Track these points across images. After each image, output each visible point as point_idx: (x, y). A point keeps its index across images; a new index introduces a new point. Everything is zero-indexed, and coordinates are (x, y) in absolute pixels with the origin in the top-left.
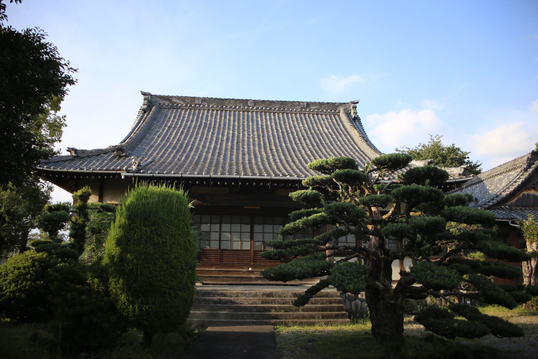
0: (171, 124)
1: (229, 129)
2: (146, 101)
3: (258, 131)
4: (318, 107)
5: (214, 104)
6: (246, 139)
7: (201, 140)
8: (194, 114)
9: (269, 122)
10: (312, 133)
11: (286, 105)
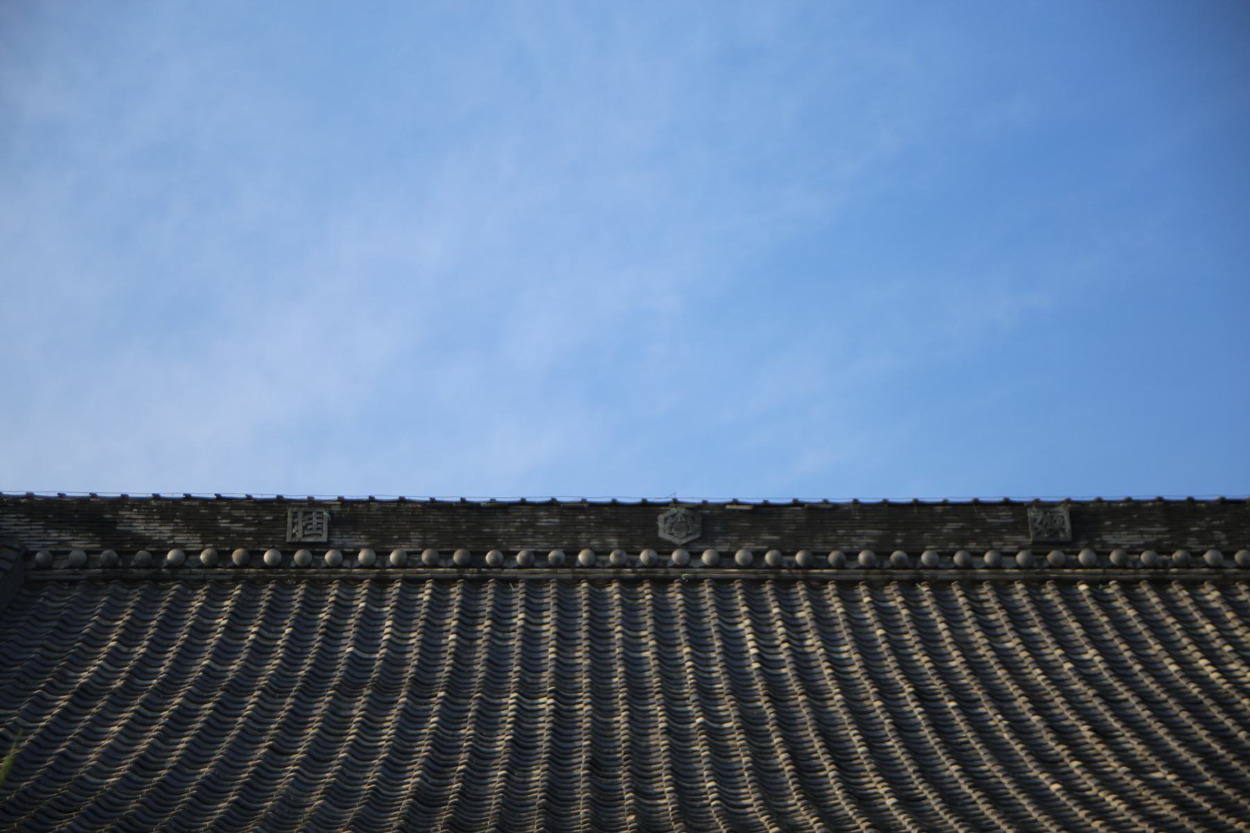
0: (103, 677)
1: (529, 690)
3: (741, 689)
4: (1157, 531)
5: (416, 538)
6: (659, 741)
9: (812, 642)
10: (1146, 698)
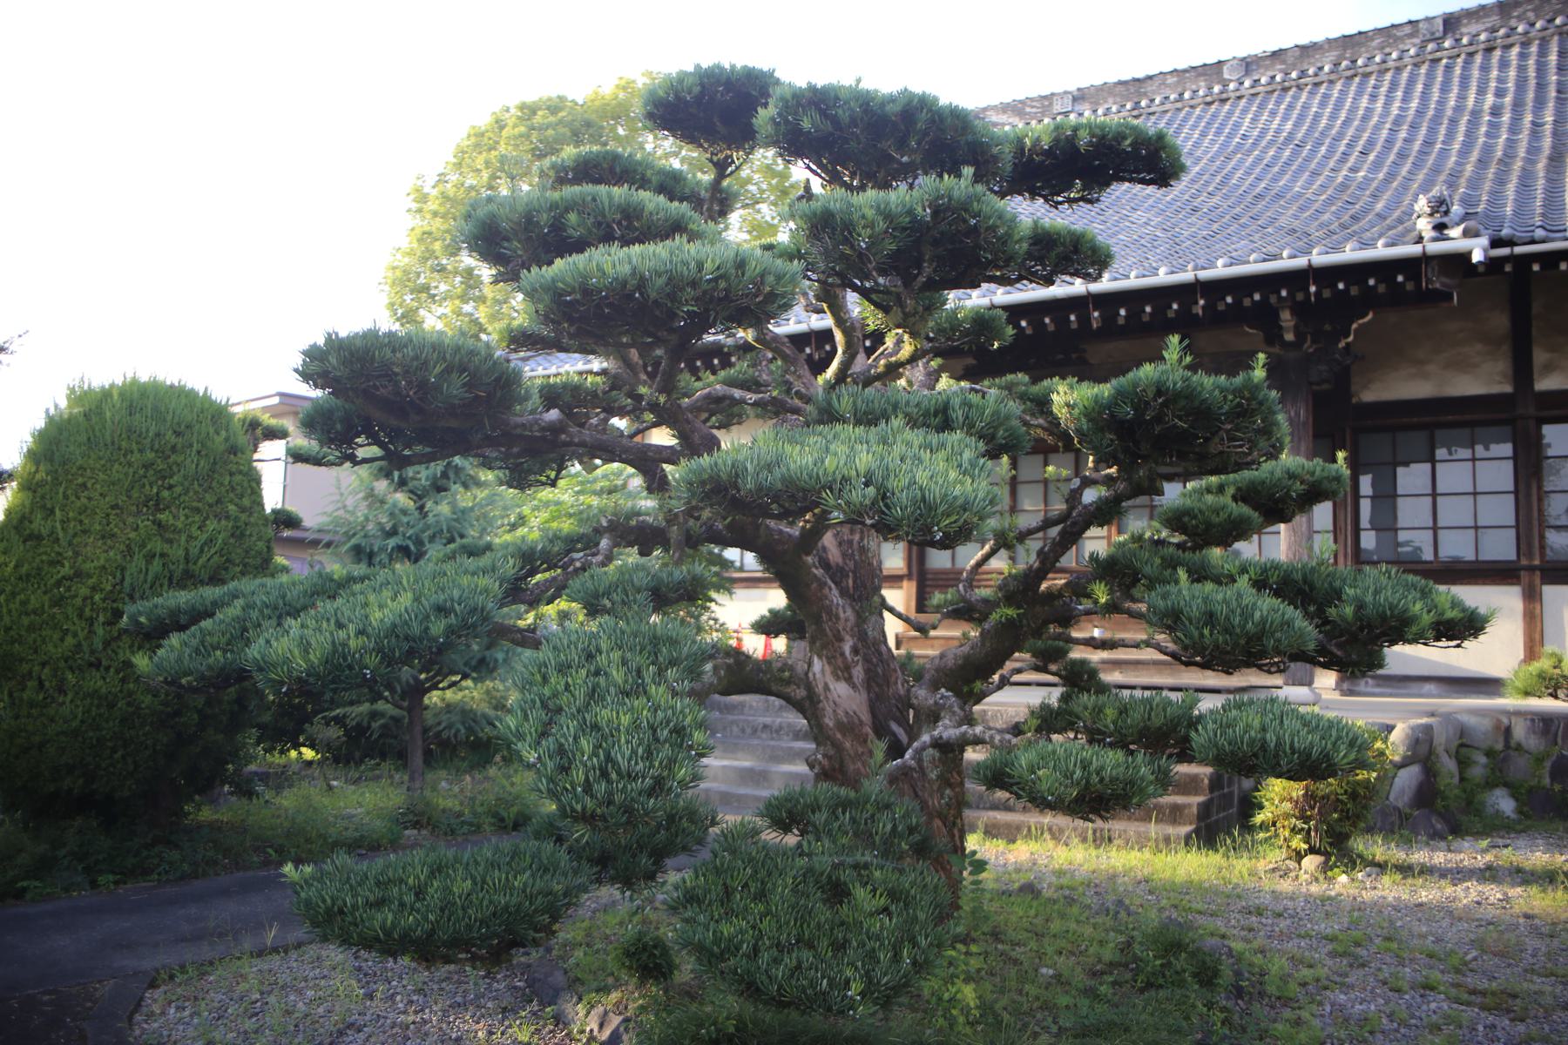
5: (1111, 100)
11: (1360, 44)
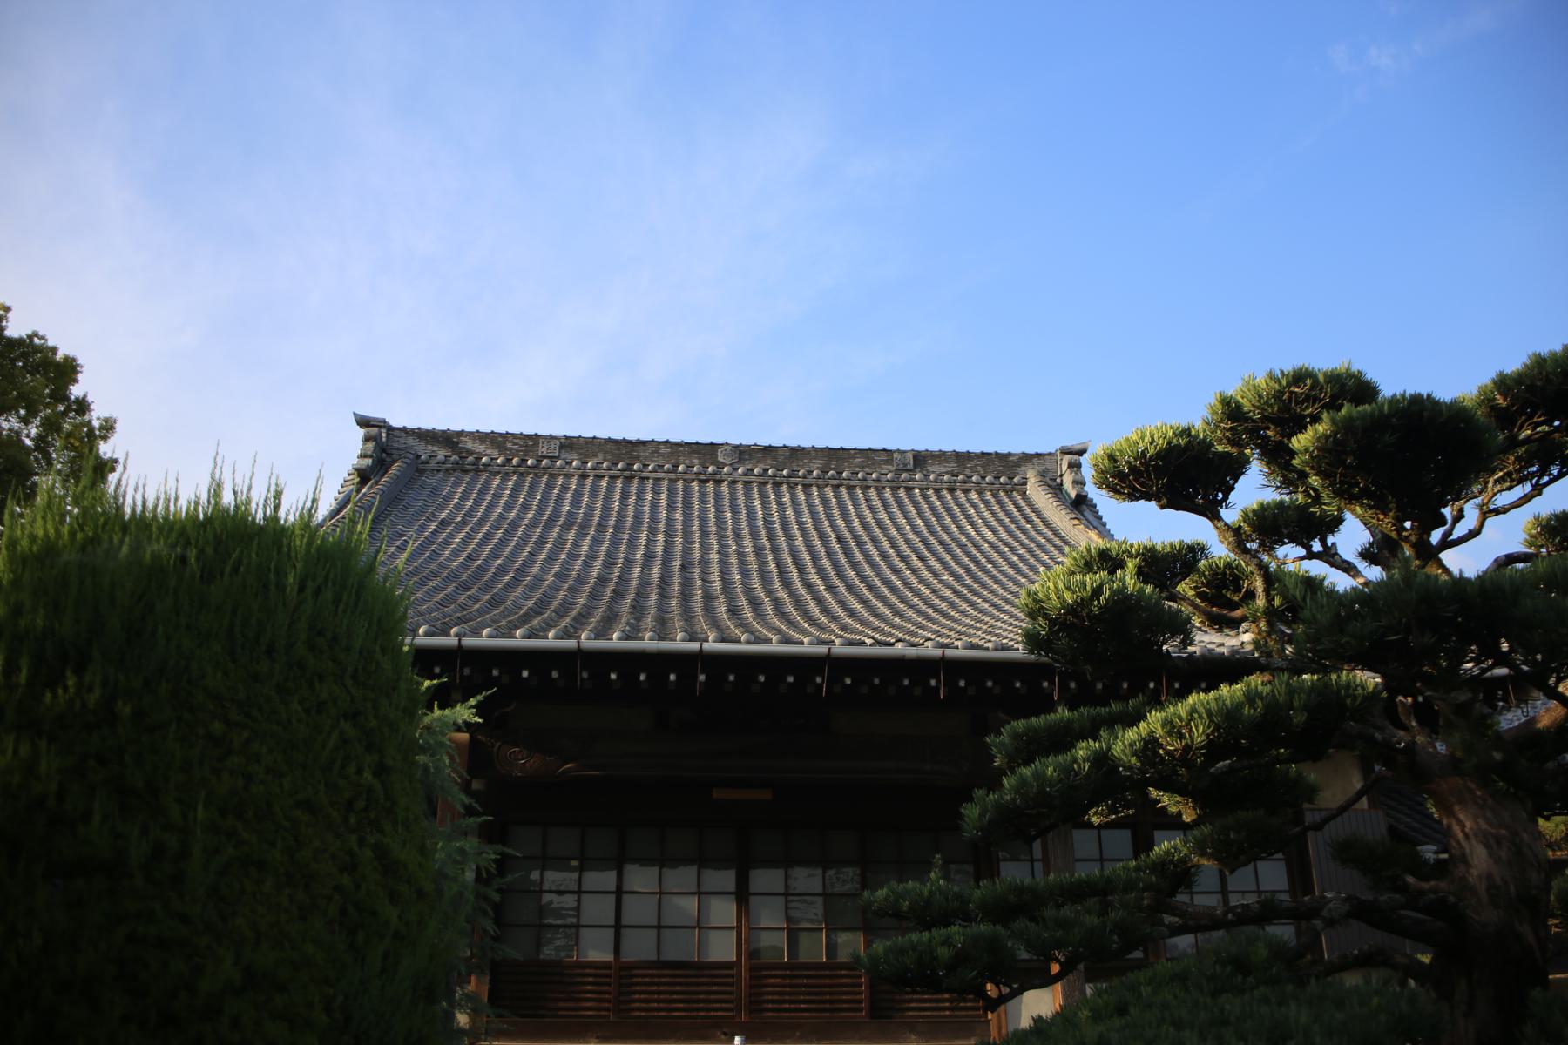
0: (452, 516)
1: (652, 531)
2: (371, 445)
3: (754, 534)
4: (952, 466)
6: (714, 557)
7: (551, 558)
8: (533, 488)
9: (790, 513)
10: (942, 543)
